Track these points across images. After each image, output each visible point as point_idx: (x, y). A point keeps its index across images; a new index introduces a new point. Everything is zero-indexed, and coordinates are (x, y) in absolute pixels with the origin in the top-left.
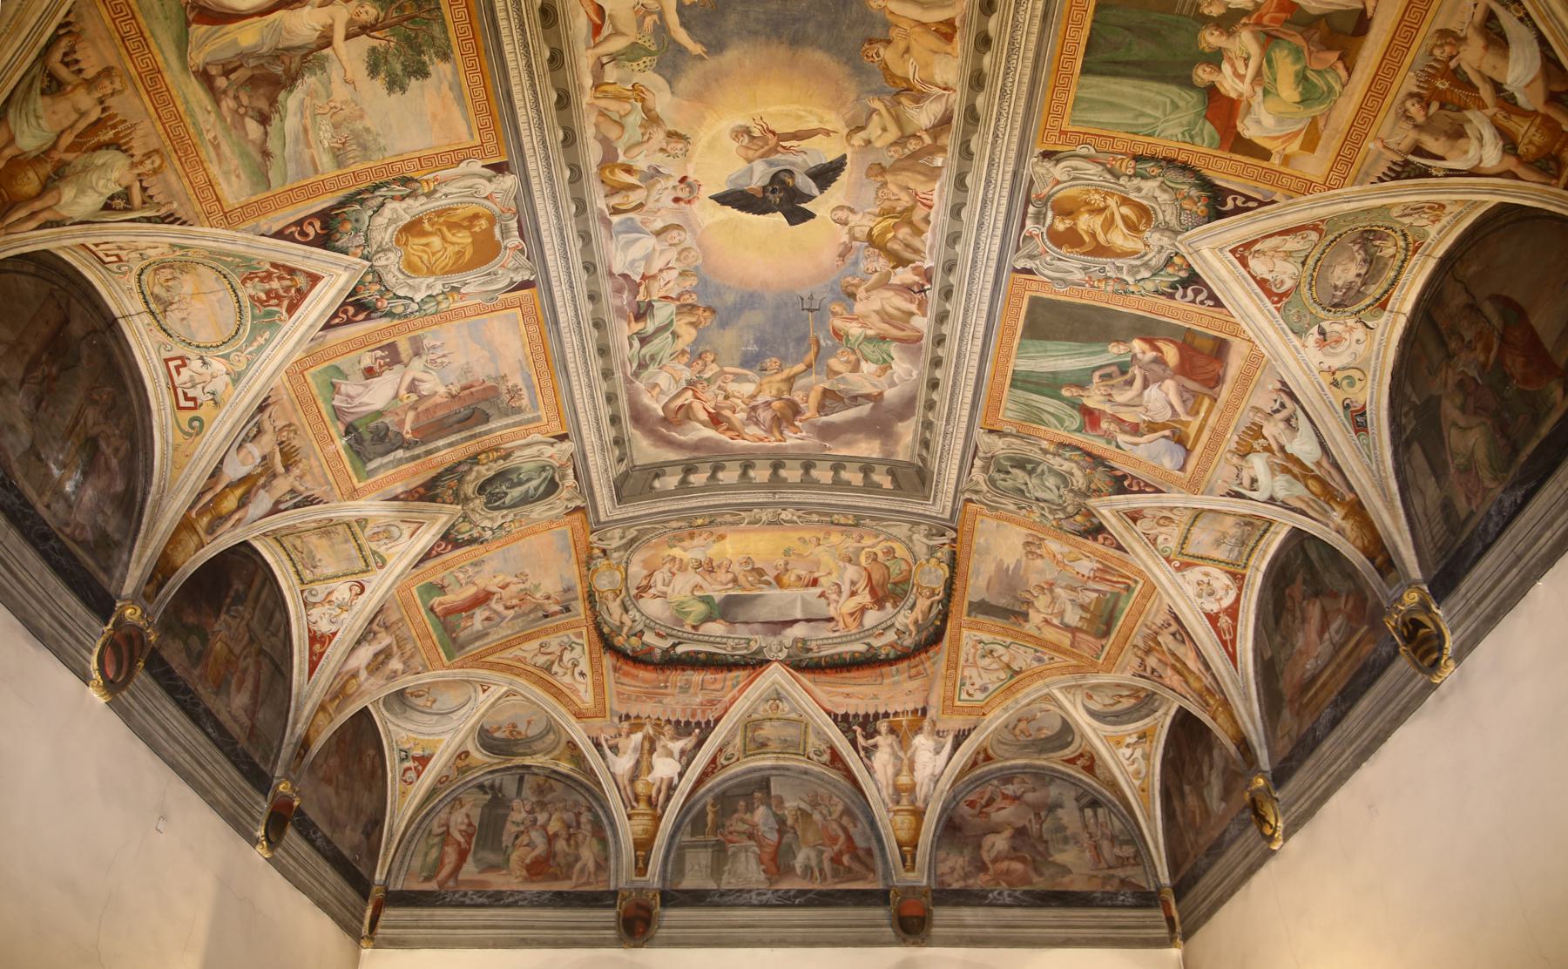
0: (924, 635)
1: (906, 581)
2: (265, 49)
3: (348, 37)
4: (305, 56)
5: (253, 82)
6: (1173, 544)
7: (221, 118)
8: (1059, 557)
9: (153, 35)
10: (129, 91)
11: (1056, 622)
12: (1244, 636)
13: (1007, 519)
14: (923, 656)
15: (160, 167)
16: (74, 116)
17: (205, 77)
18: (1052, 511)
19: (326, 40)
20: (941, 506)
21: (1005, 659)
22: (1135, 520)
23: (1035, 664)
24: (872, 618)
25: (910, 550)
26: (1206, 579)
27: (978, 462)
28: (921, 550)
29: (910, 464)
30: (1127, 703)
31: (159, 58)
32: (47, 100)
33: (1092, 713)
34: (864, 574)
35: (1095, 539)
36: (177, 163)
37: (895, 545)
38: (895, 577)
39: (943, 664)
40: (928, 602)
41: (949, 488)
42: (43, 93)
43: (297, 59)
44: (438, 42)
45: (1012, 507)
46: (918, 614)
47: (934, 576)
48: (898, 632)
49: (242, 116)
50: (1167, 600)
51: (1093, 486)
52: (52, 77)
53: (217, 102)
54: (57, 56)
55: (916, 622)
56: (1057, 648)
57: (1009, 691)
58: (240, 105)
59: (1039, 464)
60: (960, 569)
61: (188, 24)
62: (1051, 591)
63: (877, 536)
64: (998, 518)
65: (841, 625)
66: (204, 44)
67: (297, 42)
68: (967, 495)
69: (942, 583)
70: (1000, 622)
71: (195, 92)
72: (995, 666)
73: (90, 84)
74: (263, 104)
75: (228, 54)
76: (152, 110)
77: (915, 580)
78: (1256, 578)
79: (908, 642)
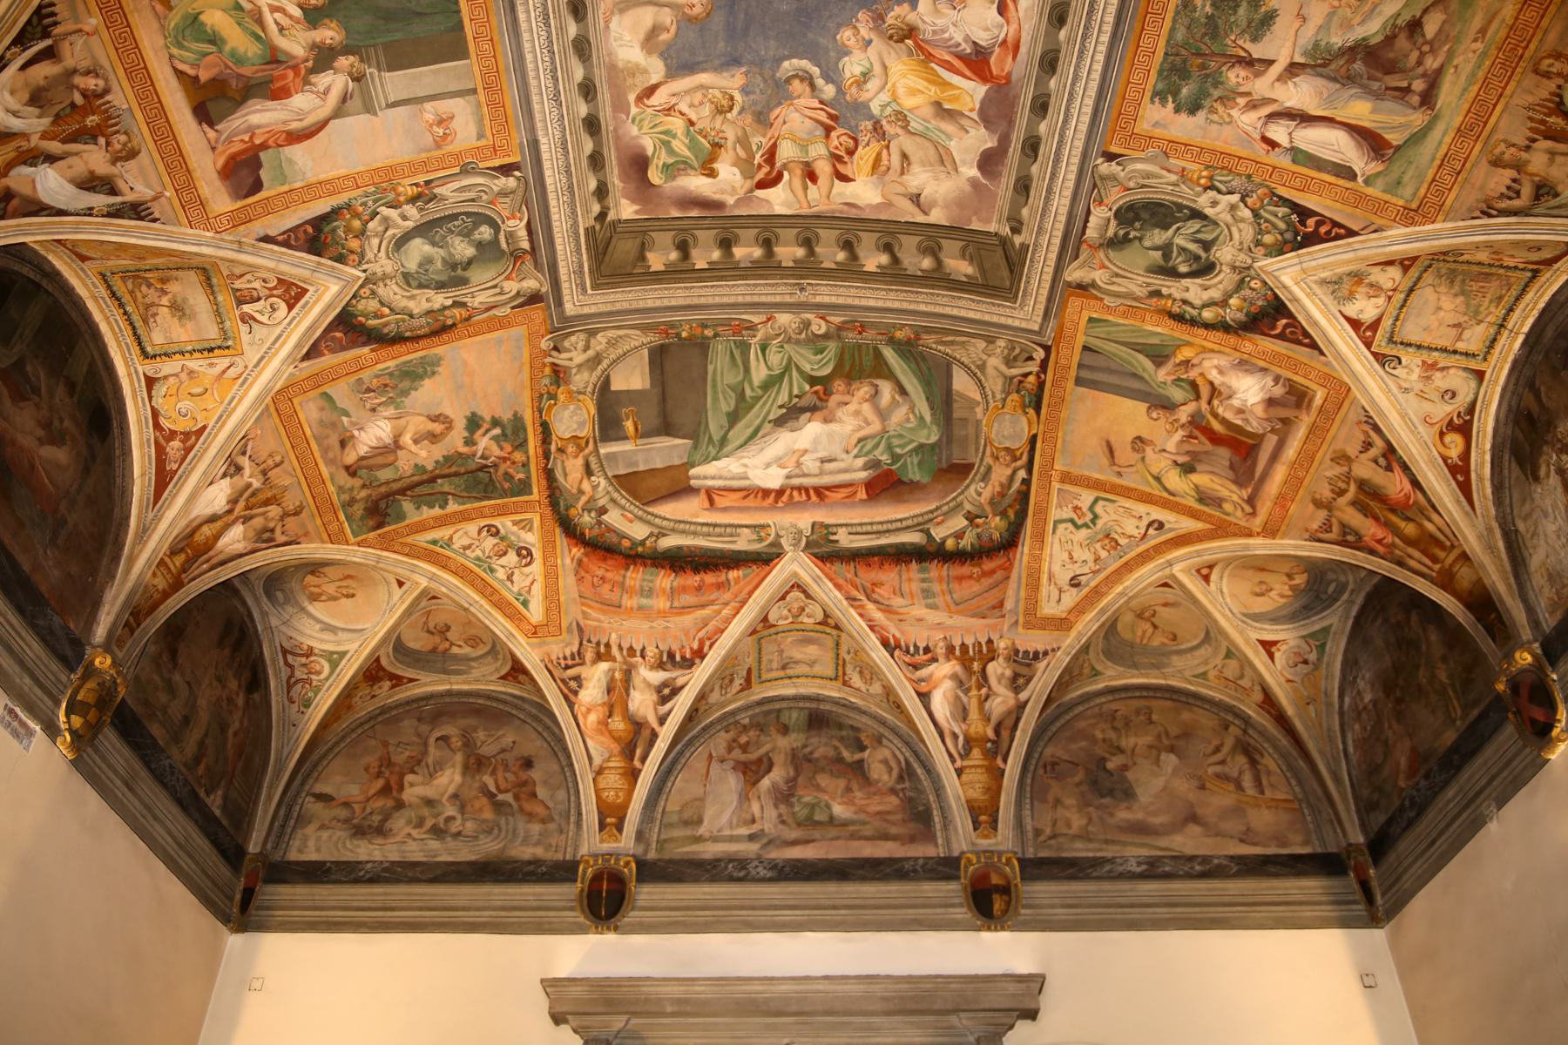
2: (1354, 91)
3: (1271, 62)
4: (1324, 66)
5: (1391, 68)
7: (1450, 55)
9: (1433, 159)
10: (1499, 136)
15: (1549, 56)
16: (1559, 159)
17: (1427, 99)
19: (1293, 69)
31: (1448, 140)
32: (1559, 188)
36: (1532, 46)
42: (1557, 195)
43: (1333, 66)
44: (1186, 21)
49: (1431, 43)
52: (1537, 197)
53: (1439, 72)
54: (1516, 203)
58: (1422, 54)
61: (1398, 148)
66: (1401, 125)
67: (1320, 82)
71: (1451, 95)
73: (1519, 166)
74: (1402, 42)
75: (1389, 104)
76: (1499, 108)
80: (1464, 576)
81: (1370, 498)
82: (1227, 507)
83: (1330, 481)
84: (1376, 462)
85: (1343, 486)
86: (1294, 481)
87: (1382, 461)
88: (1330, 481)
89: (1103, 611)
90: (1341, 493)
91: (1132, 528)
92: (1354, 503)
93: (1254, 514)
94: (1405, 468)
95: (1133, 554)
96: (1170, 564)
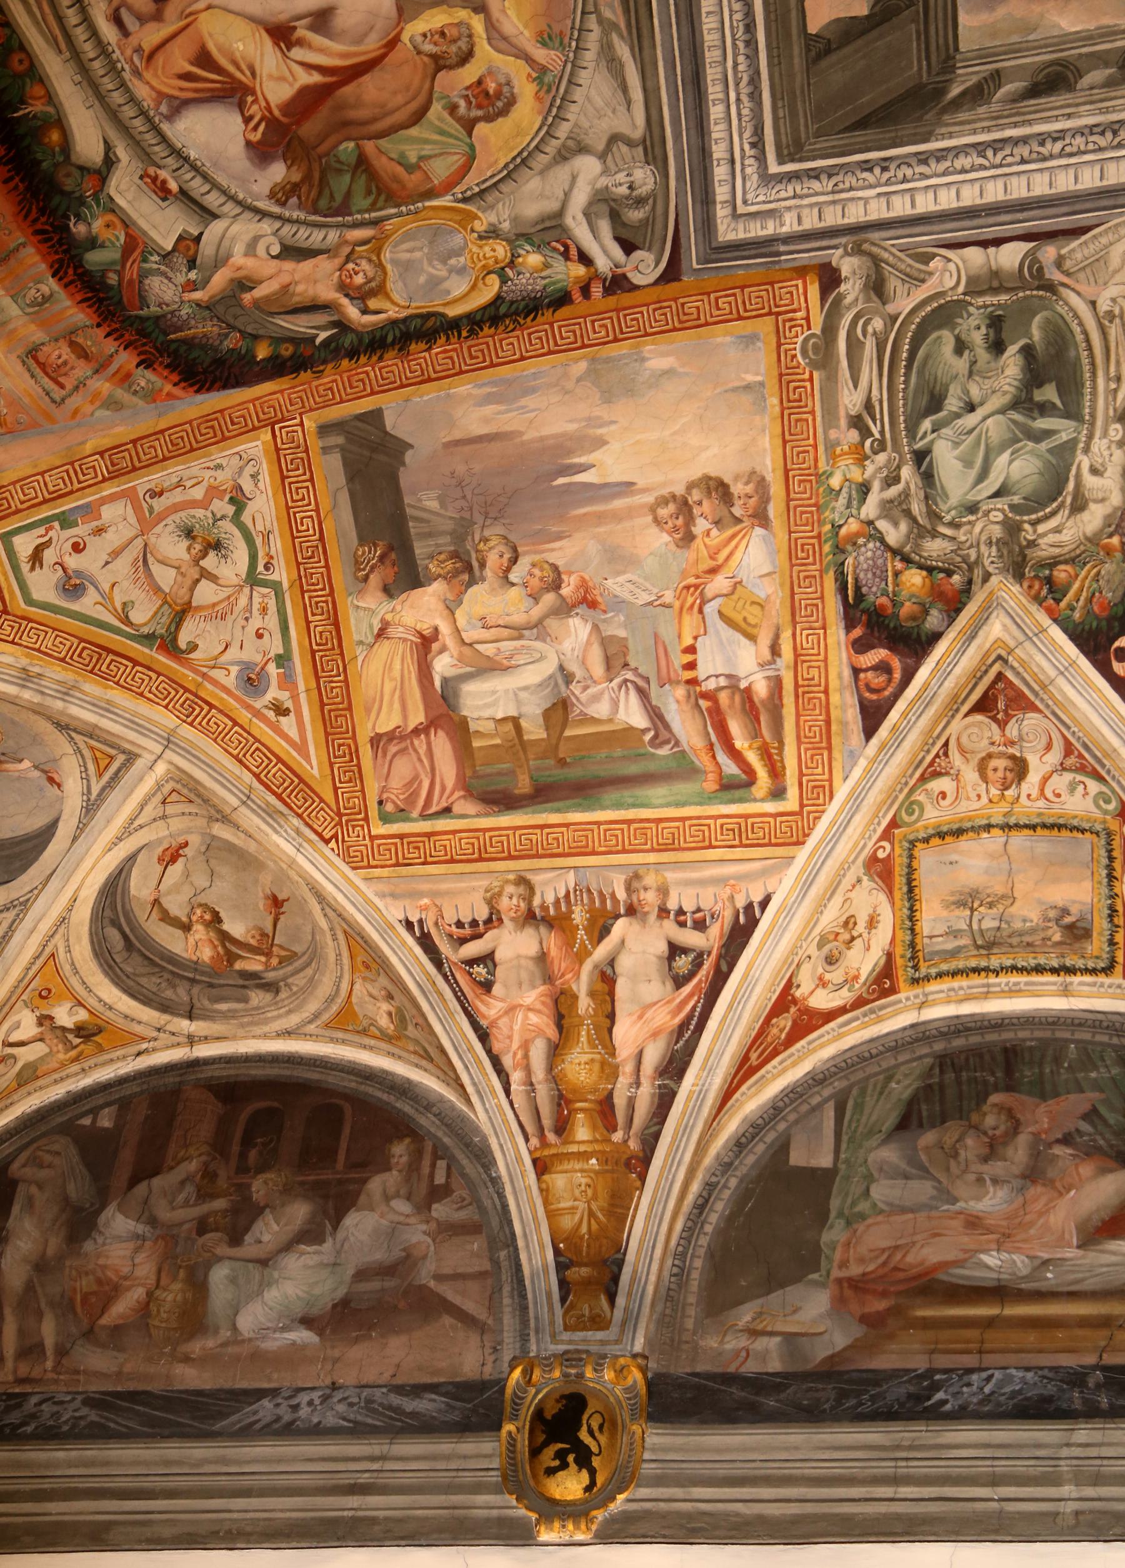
0: (209, 328)
1: (386, 193)
6: (933, 815)
8: (720, 583)
11: (443, 665)
12: (763, 1082)
13: (792, 408)
14: (126, 359)
18: (895, 509)
20: (758, 198)
21: (206, 593)
22: (984, 706)
23: (230, 679)
24: (213, 134)
25: (522, 162)
26: (861, 927)
27: (1010, 256)
28: (532, 198)
29: (948, 62)
30: (198, 947)
33: (114, 889)
34: (372, 45)
35: (860, 646)
37: (526, 113)
38: (386, 154)
39: (122, 431)
40: (327, 292)
41: (868, 203)
45: (851, 400)
46: (274, 278)
47: (433, 268)
48: (189, 244)
50: (783, 887)
51: (1061, 573)
55: (243, 284)
56: (335, 713)
57: (97, 656)
59: (1072, 412)
60: (509, 342)
62: (565, 609)
63: (544, 40)
64: (785, 378)
65: (150, 36)
68: (848, 266)
69: (421, 305)
70: (341, 523)
72: (165, 577)
77: (396, 221)
78: (899, 1017)
79: (164, 291)
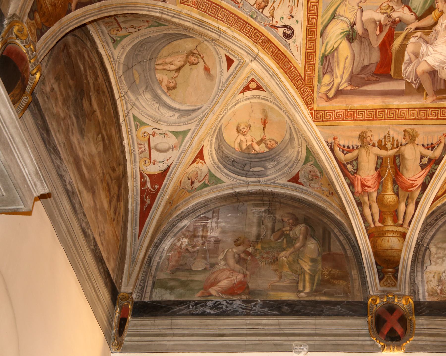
80: (391, 242)
81: (392, 167)
82: (326, 79)
83: (387, 137)
84: (422, 157)
85: (389, 145)
86: (372, 115)
87: (425, 161)
88: (387, 137)
89: (201, 23)
90: (381, 146)
91: (281, 15)
92: (379, 158)
93: (329, 99)
94: (431, 175)
95: (256, 24)
96: (256, 58)
